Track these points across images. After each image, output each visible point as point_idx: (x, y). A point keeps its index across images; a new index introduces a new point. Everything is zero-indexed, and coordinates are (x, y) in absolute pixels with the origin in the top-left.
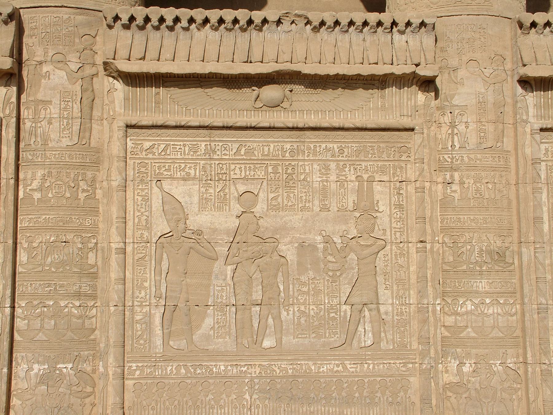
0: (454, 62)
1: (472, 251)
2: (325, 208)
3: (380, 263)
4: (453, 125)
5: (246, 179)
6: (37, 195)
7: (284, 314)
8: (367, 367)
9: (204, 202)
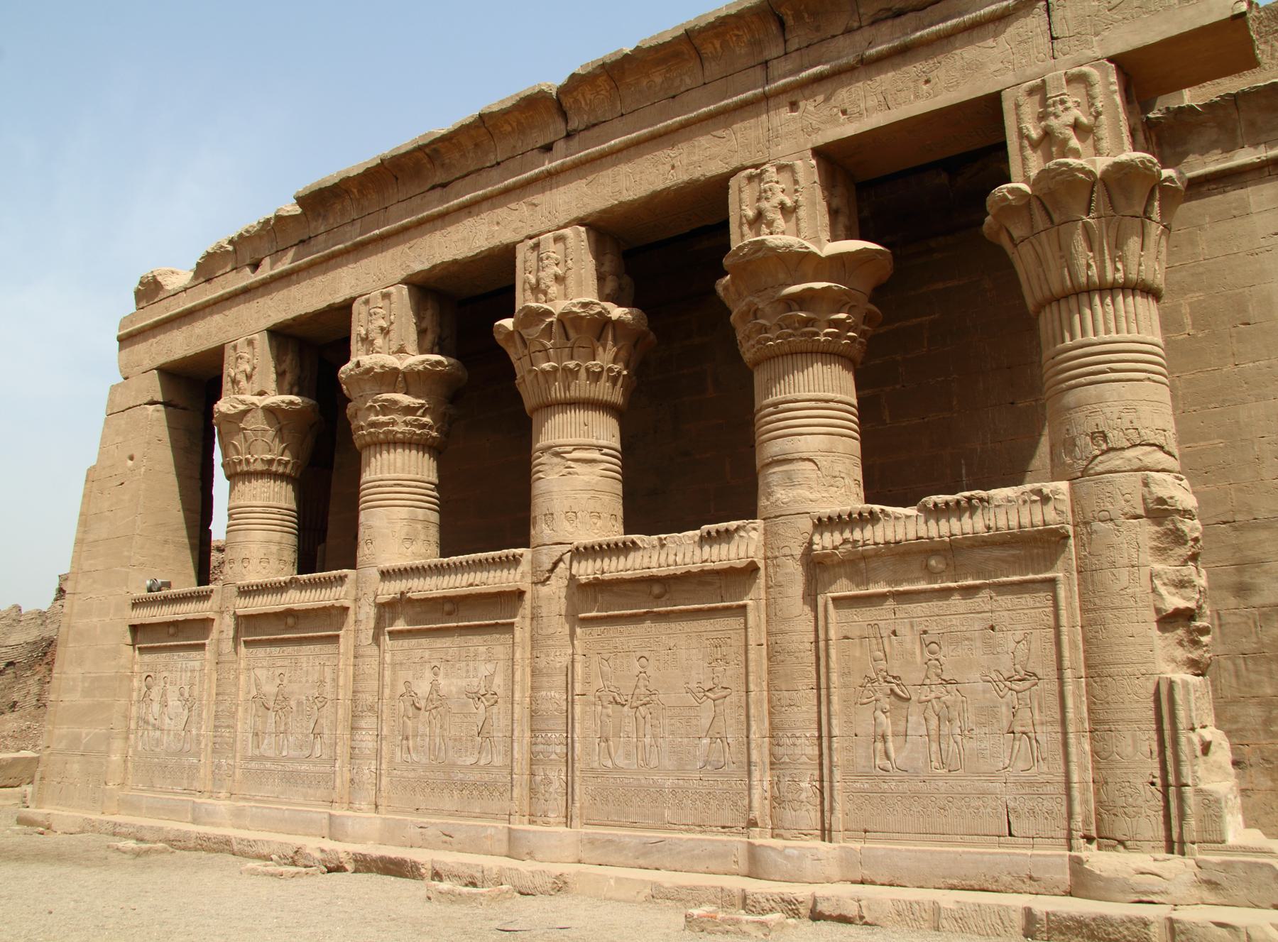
2: (307, 681)
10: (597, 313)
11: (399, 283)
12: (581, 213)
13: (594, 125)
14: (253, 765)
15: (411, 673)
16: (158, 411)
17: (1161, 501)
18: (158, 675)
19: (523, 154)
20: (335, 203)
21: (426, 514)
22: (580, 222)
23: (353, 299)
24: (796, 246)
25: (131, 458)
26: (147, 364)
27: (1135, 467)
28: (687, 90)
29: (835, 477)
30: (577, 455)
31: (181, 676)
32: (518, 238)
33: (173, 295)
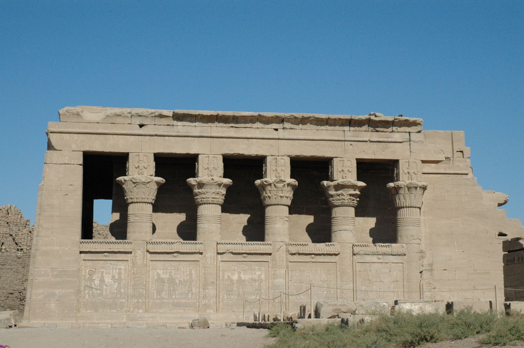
0: (207, 249)
1: (208, 282)
2: (183, 274)
3: (192, 284)
4: (206, 260)
5: (170, 269)
6: (135, 272)
7: (176, 292)
8: (190, 301)
9: (163, 273)
12: (290, 155)
13: (292, 129)
14: (157, 301)
15: (230, 273)
18: (97, 270)
19: (267, 128)
20: (188, 118)
22: (289, 156)
23: (200, 154)
25: (71, 185)
26: (74, 147)
28: (322, 130)
31: (113, 271)
32: (268, 155)
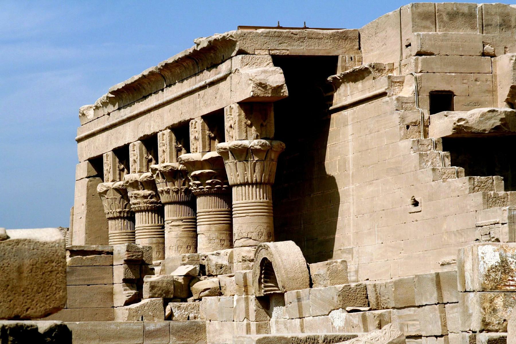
10: (170, 170)
11: (138, 140)
16: (91, 181)
17: (243, 257)
21: (157, 240)
22: (169, 128)
24: (191, 159)
27: (241, 246)
29: (211, 240)
30: (173, 223)
33: (90, 122)
